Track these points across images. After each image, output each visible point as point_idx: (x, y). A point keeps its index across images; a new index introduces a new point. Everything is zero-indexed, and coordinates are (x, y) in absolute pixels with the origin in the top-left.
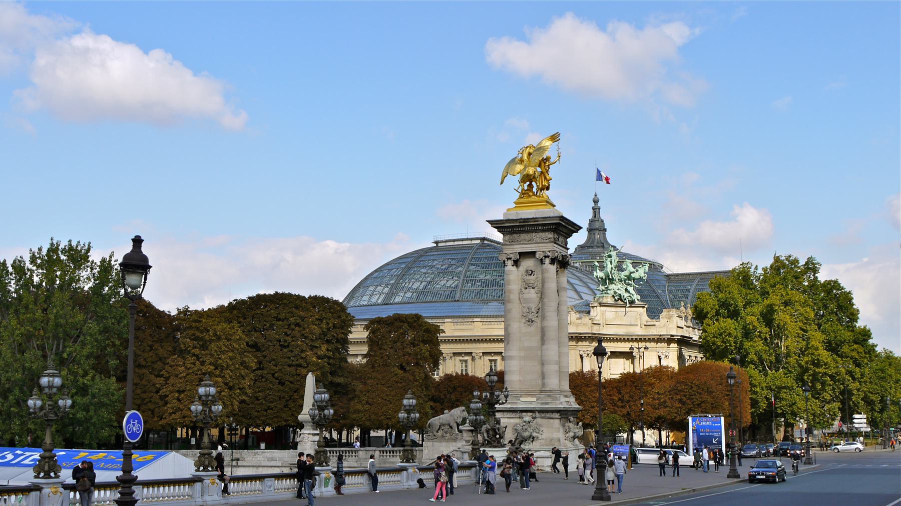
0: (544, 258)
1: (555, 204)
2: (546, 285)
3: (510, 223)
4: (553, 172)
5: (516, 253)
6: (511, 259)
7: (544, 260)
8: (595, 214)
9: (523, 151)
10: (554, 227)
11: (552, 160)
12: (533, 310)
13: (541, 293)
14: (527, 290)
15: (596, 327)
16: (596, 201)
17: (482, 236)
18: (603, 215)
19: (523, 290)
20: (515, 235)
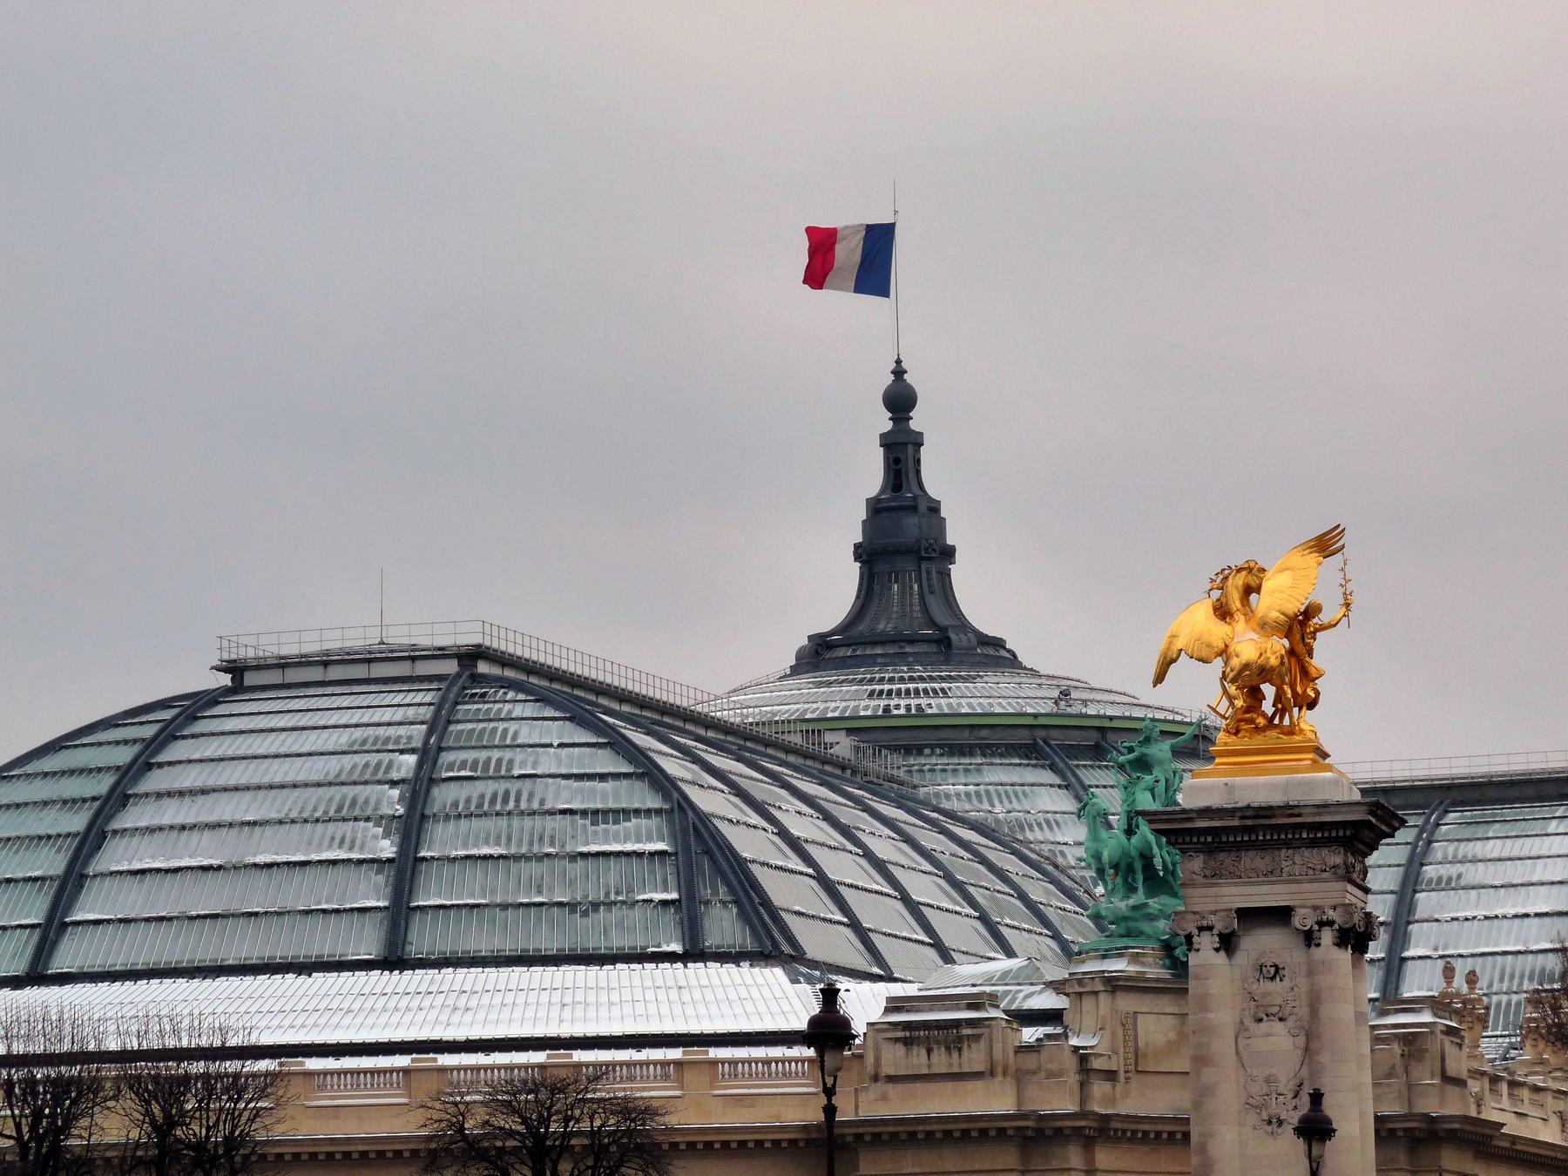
0: (1316, 927)
1: (1327, 749)
2: (1325, 1012)
3: (1212, 819)
4: (1325, 652)
5: (1231, 910)
6: (1210, 928)
7: (1316, 934)
9: (1226, 578)
10: (1348, 833)
11: (1324, 617)
12: (1282, 1089)
13: (1307, 1036)
14: (1262, 1025)
15: (1099, 1088)
16: (900, 401)
17: (468, 637)
18: (935, 477)
19: (1249, 1022)
20: (1222, 856)
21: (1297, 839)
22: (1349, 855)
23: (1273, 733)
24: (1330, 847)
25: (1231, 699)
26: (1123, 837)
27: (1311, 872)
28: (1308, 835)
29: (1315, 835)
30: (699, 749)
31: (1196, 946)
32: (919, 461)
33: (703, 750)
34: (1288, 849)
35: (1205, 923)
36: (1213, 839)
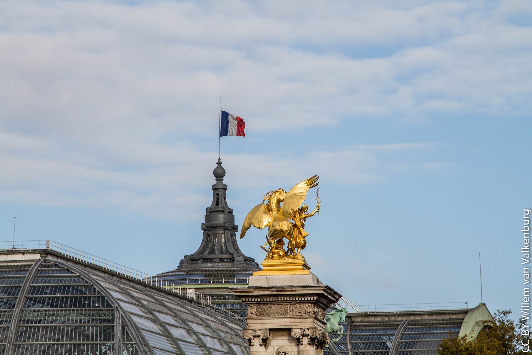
0: (301, 337)
5: (266, 329)
6: (258, 336)
8: (218, 199)
10: (315, 299)
11: (310, 211)
16: (219, 174)
20: (264, 307)
21: (294, 301)
22: (315, 308)
23: (286, 258)
24: (308, 304)
25: (270, 244)
27: (300, 314)
30: (130, 290)
31: (252, 344)
32: (225, 195)
33: (131, 290)
34: (291, 304)
35: (256, 334)
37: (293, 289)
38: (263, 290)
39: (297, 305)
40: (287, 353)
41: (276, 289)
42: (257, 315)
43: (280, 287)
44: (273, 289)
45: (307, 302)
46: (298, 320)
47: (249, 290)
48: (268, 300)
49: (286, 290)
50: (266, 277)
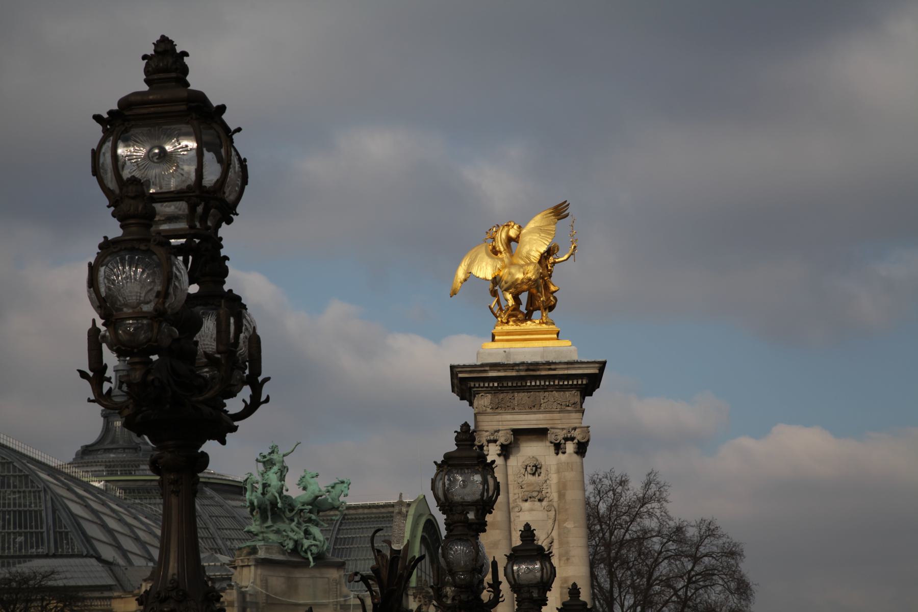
0: (563, 441)
3: (499, 371)
7: (562, 446)
10: (584, 382)
20: (501, 396)
21: (552, 385)
26: (260, 496)
28: (559, 382)
29: (563, 382)
34: (545, 392)
36: (498, 384)
37: (553, 367)
38: (505, 368)
39: (554, 392)
40: (538, 467)
41: (525, 367)
42: (492, 408)
43: (531, 364)
44: (521, 368)
45: (572, 387)
46: (556, 416)
47: (482, 369)
48: (510, 384)
49: (542, 369)
50: (505, 350)
